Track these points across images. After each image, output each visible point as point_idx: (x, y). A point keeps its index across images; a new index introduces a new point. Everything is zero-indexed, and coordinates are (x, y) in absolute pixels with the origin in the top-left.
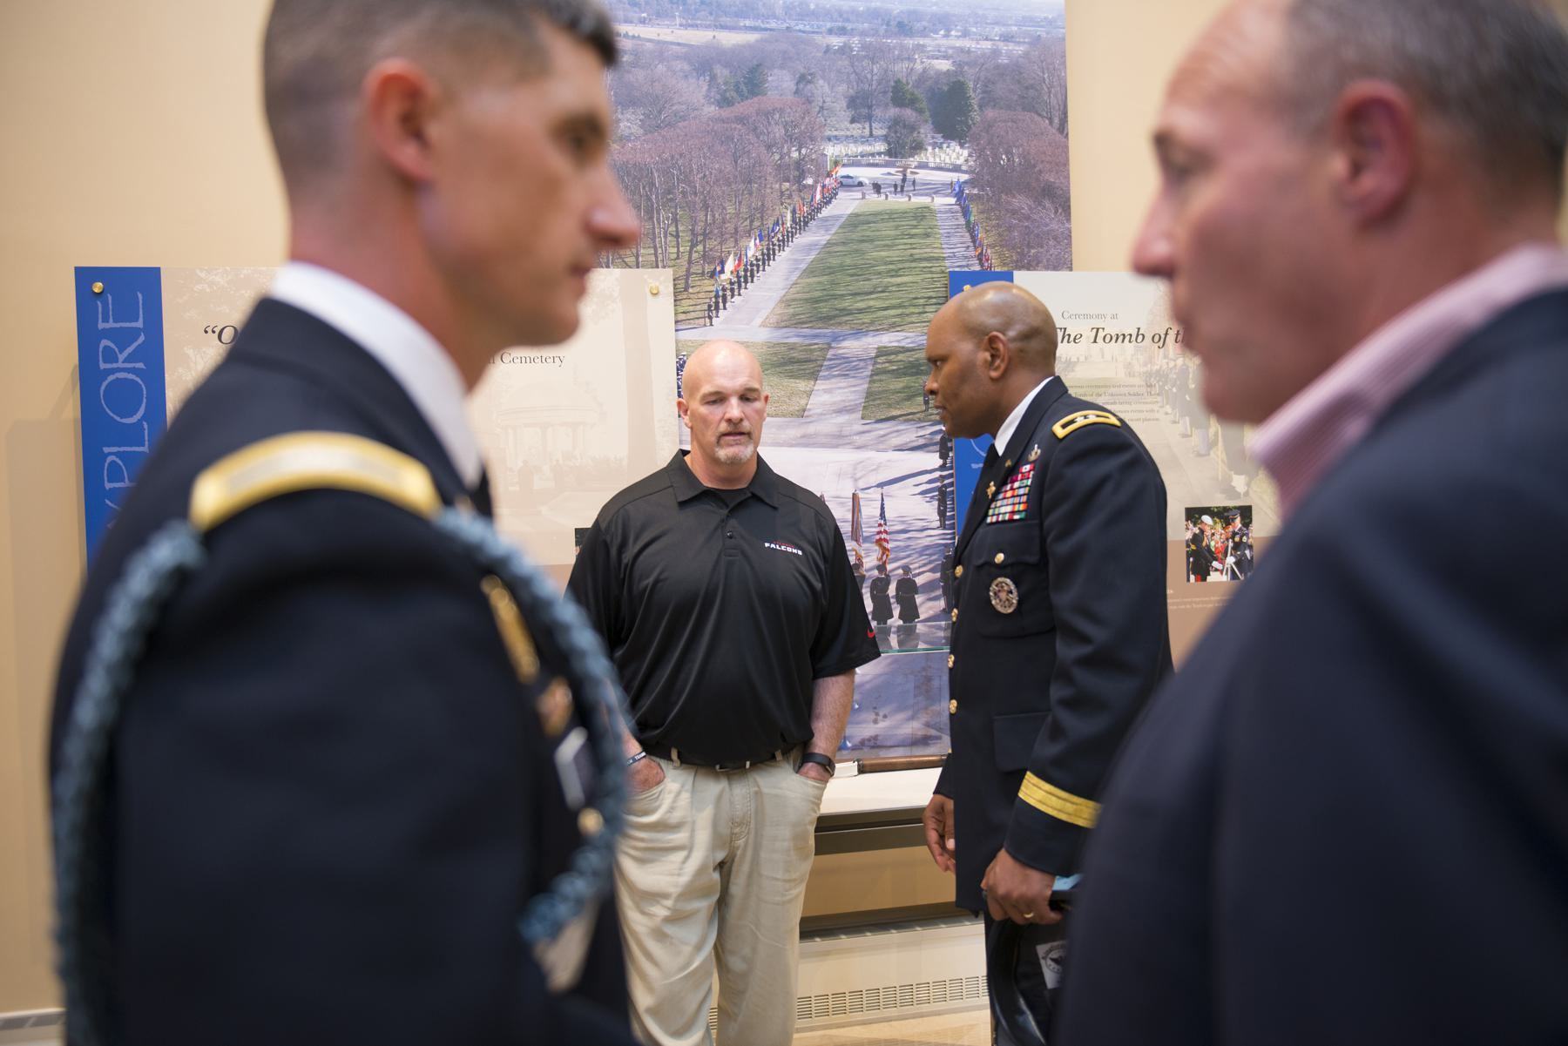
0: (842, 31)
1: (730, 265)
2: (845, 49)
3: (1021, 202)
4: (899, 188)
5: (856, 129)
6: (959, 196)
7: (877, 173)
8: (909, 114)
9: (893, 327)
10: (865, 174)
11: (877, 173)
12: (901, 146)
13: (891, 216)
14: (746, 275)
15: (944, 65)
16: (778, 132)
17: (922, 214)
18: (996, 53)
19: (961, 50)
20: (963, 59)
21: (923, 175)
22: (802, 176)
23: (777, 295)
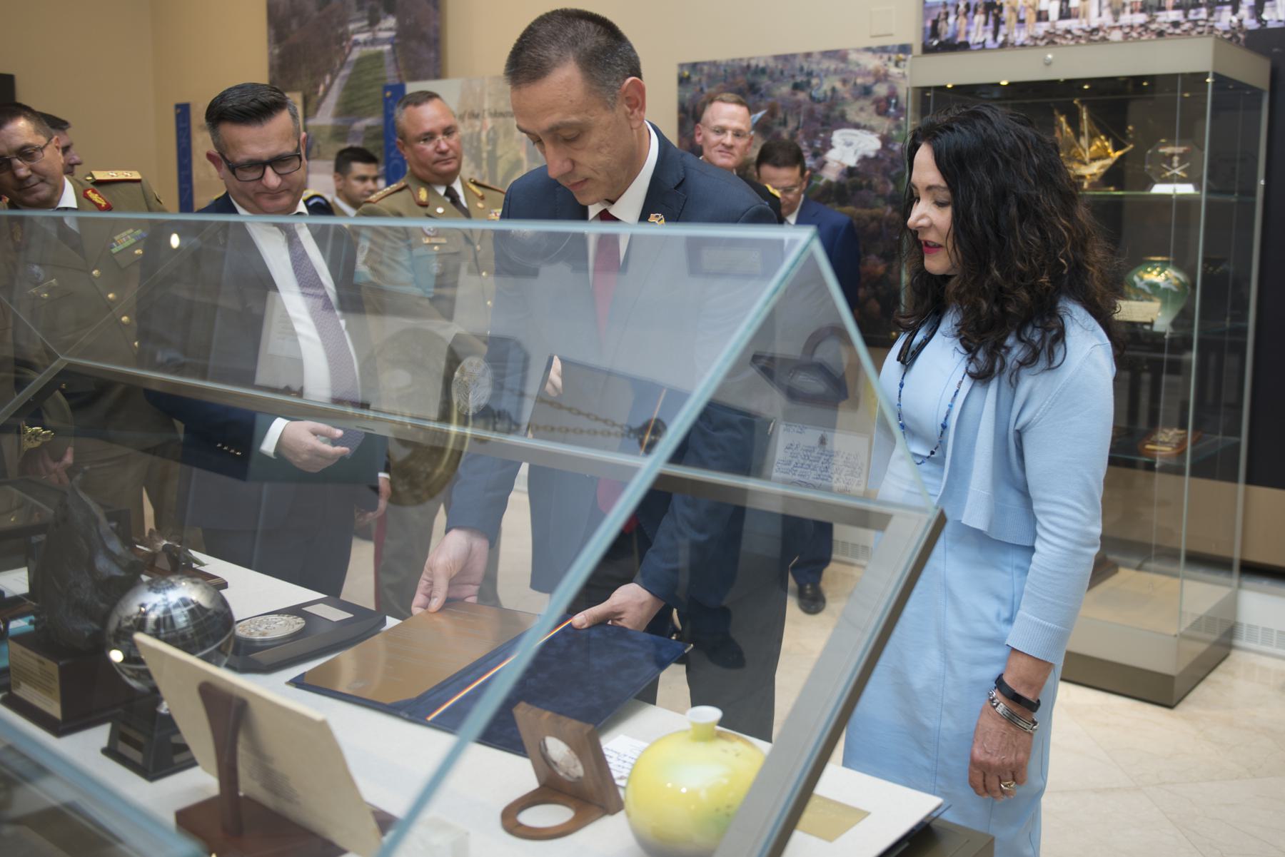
3: (413, 44)
6: (392, 43)
10: (361, 37)
12: (374, 22)
17: (379, 55)
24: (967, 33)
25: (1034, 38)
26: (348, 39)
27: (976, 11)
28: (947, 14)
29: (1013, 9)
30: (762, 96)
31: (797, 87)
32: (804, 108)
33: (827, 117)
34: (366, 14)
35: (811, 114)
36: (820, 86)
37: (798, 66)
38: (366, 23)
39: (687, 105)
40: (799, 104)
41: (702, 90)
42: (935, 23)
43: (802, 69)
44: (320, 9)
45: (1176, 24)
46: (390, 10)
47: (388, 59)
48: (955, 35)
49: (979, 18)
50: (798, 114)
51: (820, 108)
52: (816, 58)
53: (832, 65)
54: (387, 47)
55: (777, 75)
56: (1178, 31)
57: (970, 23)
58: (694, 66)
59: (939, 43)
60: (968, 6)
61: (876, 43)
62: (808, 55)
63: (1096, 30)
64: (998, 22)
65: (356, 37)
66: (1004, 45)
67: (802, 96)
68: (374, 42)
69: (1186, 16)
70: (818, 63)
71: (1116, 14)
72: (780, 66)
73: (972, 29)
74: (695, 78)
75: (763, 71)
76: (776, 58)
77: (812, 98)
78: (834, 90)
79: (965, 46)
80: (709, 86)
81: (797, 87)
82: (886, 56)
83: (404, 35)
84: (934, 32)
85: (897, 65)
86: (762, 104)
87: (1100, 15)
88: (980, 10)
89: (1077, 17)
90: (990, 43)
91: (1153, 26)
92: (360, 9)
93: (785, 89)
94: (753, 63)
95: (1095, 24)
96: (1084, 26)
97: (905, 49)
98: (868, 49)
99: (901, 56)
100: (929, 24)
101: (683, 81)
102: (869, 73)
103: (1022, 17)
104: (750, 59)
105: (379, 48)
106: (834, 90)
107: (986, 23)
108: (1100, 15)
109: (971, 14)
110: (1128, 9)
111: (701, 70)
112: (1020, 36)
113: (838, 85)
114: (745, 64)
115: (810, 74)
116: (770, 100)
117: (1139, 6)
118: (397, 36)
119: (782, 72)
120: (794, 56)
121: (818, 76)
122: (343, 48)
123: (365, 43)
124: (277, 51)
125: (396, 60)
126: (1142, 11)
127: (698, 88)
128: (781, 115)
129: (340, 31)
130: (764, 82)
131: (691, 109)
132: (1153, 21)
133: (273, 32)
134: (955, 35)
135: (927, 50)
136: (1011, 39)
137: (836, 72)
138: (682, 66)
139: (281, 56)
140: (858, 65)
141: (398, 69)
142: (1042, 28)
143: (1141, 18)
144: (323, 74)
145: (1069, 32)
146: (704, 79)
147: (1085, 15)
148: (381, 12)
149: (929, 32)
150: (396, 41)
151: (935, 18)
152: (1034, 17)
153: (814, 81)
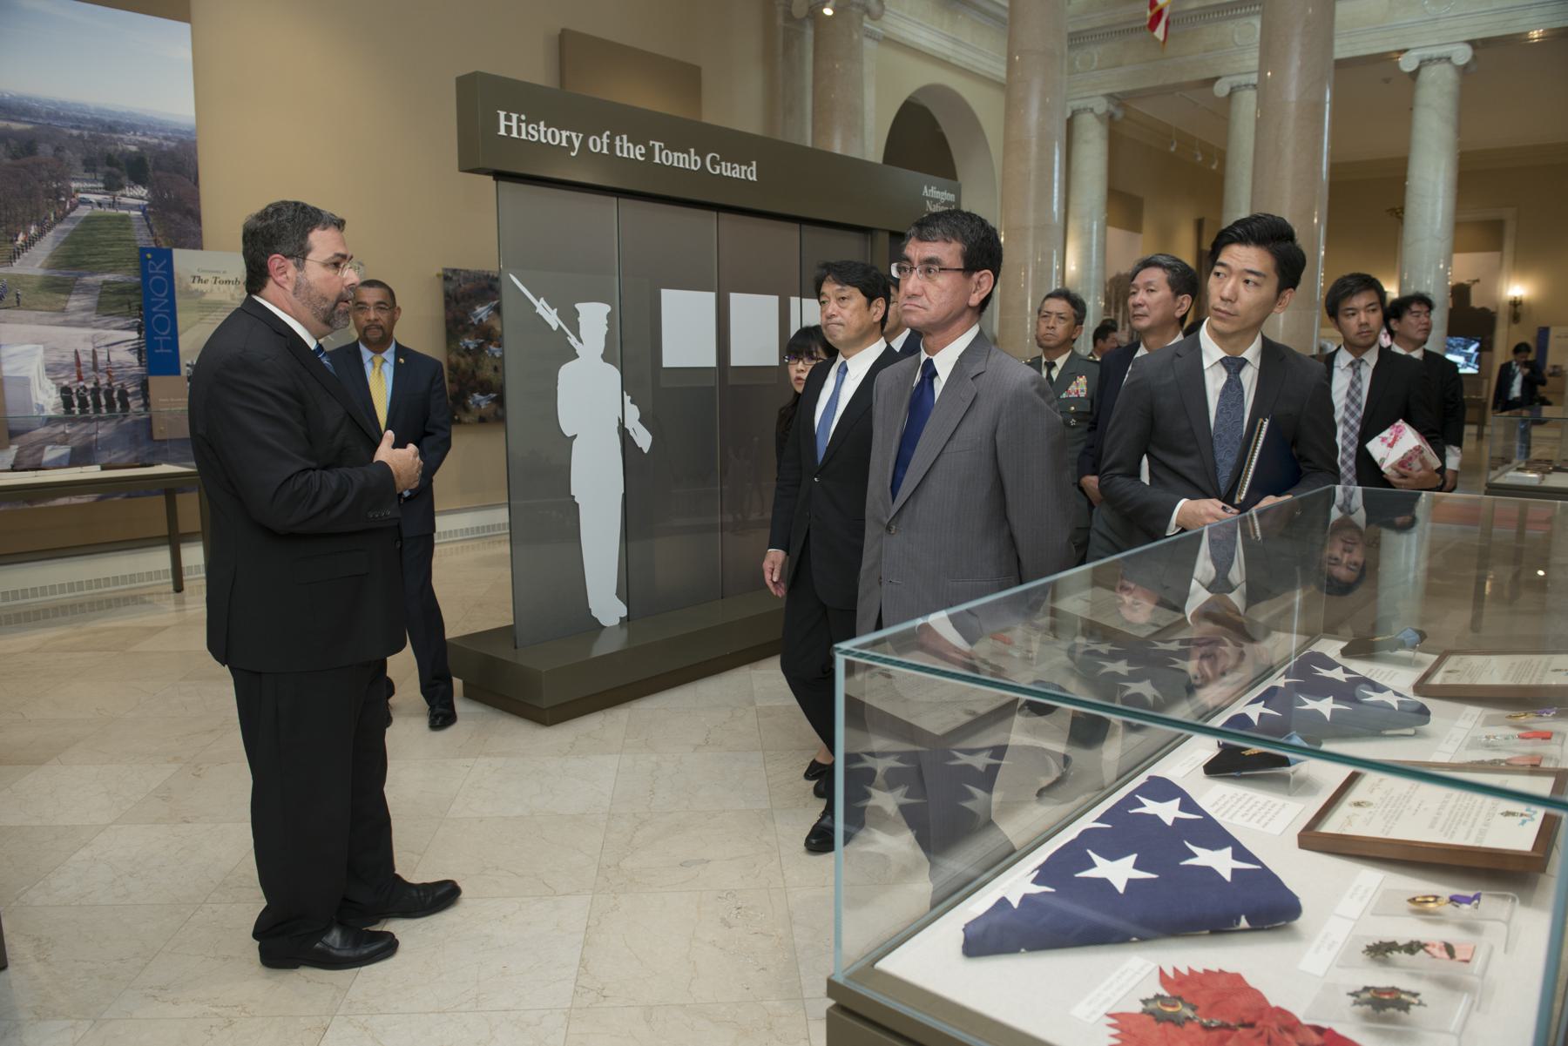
0: (78, 128)
1: (21, 237)
2: (80, 137)
3: (176, 216)
4: (112, 205)
5: (87, 176)
7: (99, 197)
8: (115, 170)
9: (110, 271)
10: (93, 198)
11: (99, 197)
12: (112, 185)
13: (108, 218)
14: (30, 243)
15: (133, 148)
16: (45, 174)
17: (124, 218)
18: (160, 145)
21: (124, 200)
22: (59, 196)
23: (47, 253)
144: (25, 225)
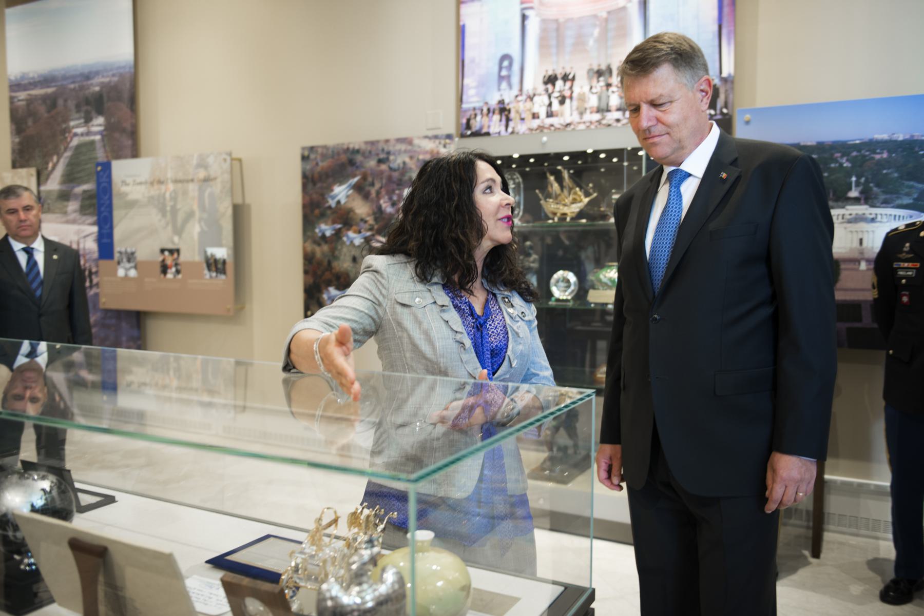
0: (74, 82)
2: (74, 89)
3: (117, 135)
8: (89, 108)
10: (79, 130)
12: (88, 120)
15: (97, 89)
17: (92, 143)
18: (110, 82)
19: (102, 83)
20: (103, 85)
24: (489, 127)
25: (531, 130)
26: (70, 132)
27: (494, 113)
28: (476, 115)
29: (517, 112)
30: (357, 167)
31: (380, 161)
32: (386, 174)
33: (400, 180)
34: (82, 114)
35: (390, 179)
36: (395, 160)
37: (380, 148)
38: (82, 121)
39: (308, 173)
40: (382, 172)
41: (317, 164)
42: (468, 120)
43: (383, 150)
44: (49, 112)
45: (618, 120)
46: (100, 112)
47: (99, 146)
48: (481, 128)
49: (496, 117)
50: (381, 179)
51: (396, 175)
52: (392, 142)
53: (403, 147)
54: (98, 137)
55: (367, 153)
56: (619, 125)
57: (490, 120)
58: (312, 149)
59: (468, 130)
60: (489, 110)
61: (430, 134)
62: (387, 141)
63: (568, 125)
64: (508, 120)
65: (75, 130)
66: (512, 133)
67: (384, 167)
68: (88, 133)
69: (624, 114)
70: (394, 146)
71: (581, 114)
72: (369, 148)
73: (492, 124)
74: (312, 156)
75: (358, 151)
76: (366, 143)
77: (391, 169)
78: (404, 163)
79: (488, 134)
80: (322, 161)
81: (380, 161)
82: (437, 141)
83: (110, 130)
84: (468, 126)
85: (445, 146)
86: (358, 172)
87: (571, 115)
88: (497, 112)
89: (557, 116)
90: (503, 132)
91: (604, 122)
92: (78, 111)
93: (372, 163)
94: (351, 146)
95: (568, 121)
96: (562, 122)
97: (449, 137)
98: (426, 137)
99: (448, 141)
100: (464, 121)
101: (304, 158)
102: (426, 152)
103: (523, 116)
104: (349, 143)
105: (92, 138)
106: (404, 163)
107: (501, 120)
108: (571, 115)
109: (491, 114)
110: (588, 111)
111: (317, 152)
112: (522, 128)
113: (407, 160)
114: (345, 147)
115: (389, 153)
116: (363, 170)
117: (595, 109)
118: (105, 130)
119: (370, 152)
120: (378, 142)
121: (394, 154)
122: (66, 138)
123: (82, 135)
124: (17, 140)
125: (104, 146)
126: (598, 111)
127: (314, 163)
128: (370, 179)
129: (64, 126)
130: (359, 158)
131: (310, 176)
132: (603, 118)
133: (14, 127)
134: (481, 128)
135: (463, 136)
136: (516, 130)
137: (405, 151)
138: (303, 149)
139: (20, 143)
140: (419, 147)
141: (106, 151)
142: (535, 123)
143: (597, 117)
145: (552, 125)
146: (319, 158)
147: (562, 115)
148: (93, 114)
149: (464, 126)
150: (105, 133)
151: (468, 117)
152: (530, 116)
153: (392, 158)
